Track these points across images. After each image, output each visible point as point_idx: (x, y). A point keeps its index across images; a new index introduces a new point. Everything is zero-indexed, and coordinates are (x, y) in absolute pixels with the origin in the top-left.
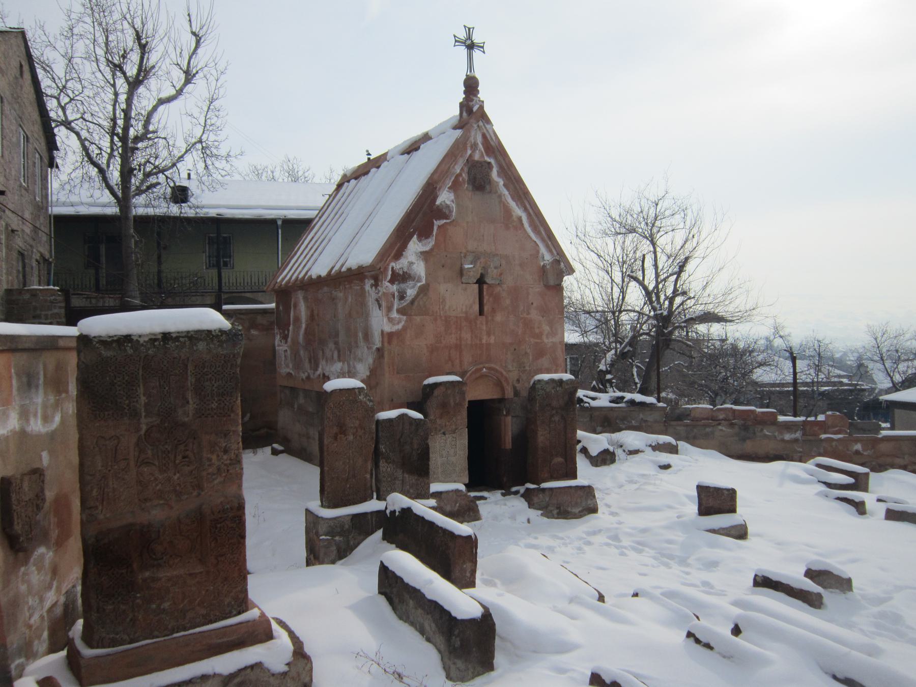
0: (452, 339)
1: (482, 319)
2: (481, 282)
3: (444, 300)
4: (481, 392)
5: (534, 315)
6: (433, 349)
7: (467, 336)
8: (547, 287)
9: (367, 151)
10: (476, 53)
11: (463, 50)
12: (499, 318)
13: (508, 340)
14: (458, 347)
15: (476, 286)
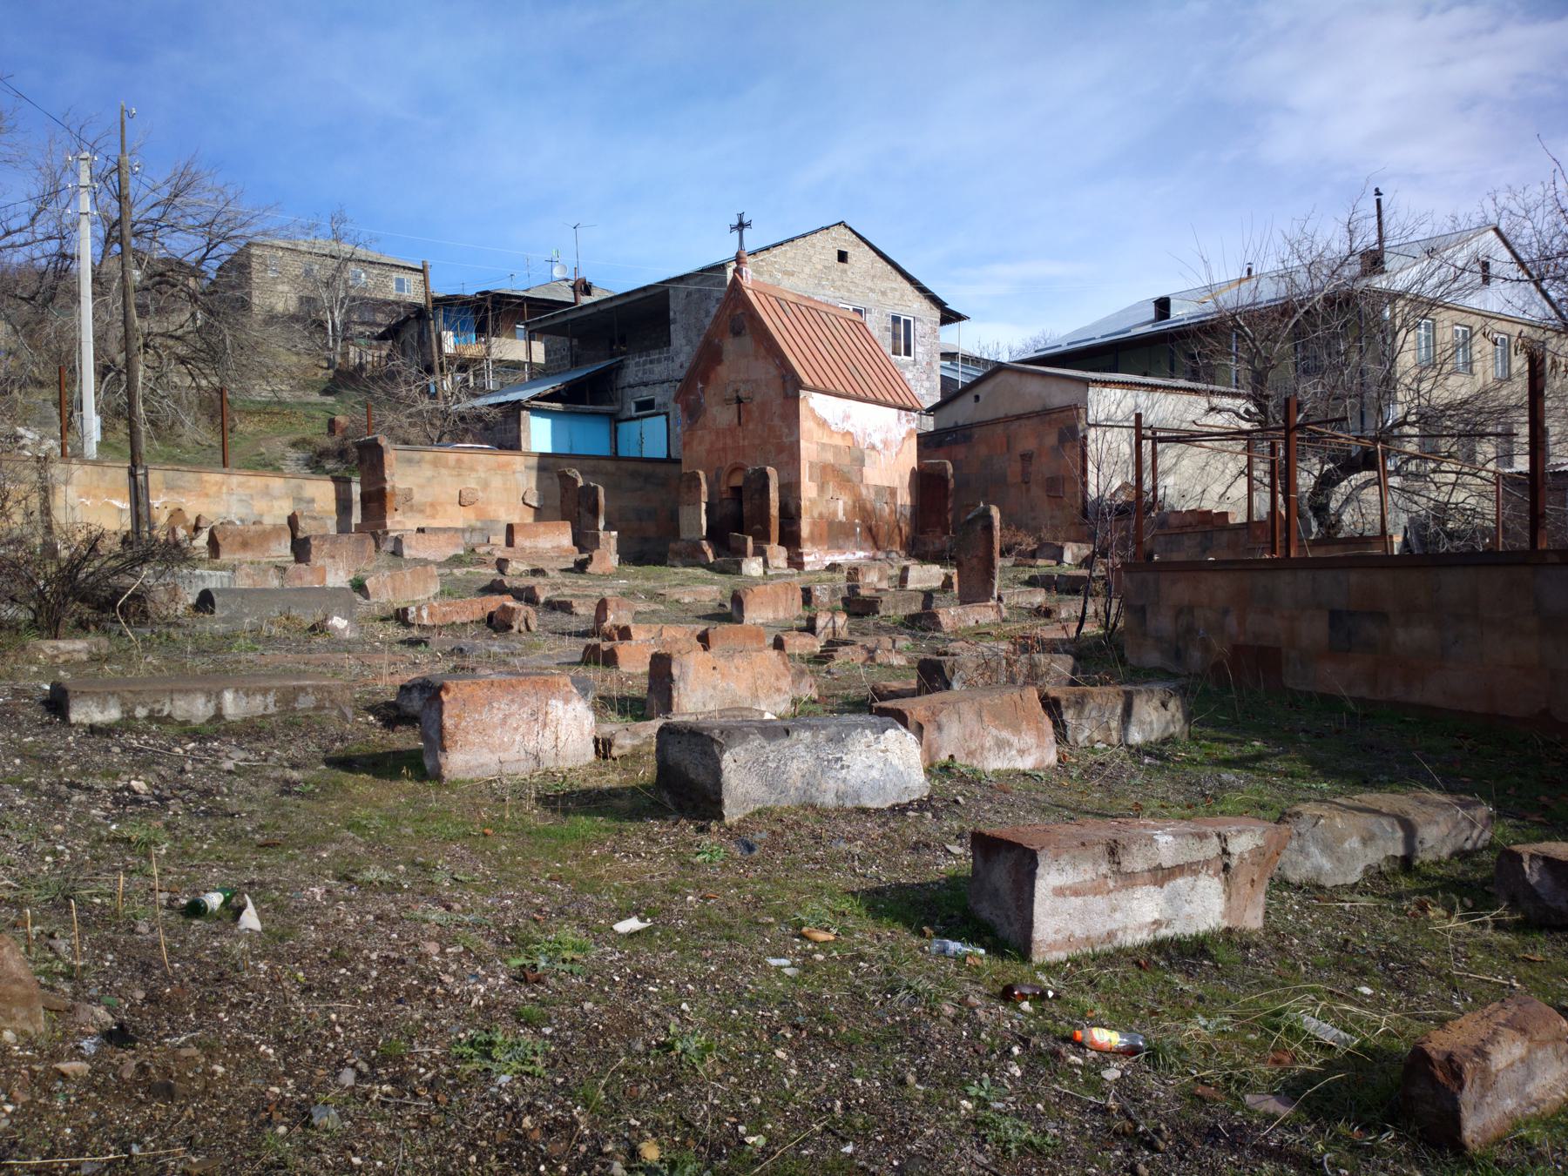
0: (720, 445)
1: (740, 429)
2: (739, 401)
3: (715, 420)
4: (737, 481)
5: (777, 422)
6: (709, 452)
7: (729, 441)
8: (786, 397)
9: (1377, 190)
10: (746, 231)
11: (736, 233)
12: (751, 426)
13: (757, 442)
14: (724, 449)
15: (735, 406)
